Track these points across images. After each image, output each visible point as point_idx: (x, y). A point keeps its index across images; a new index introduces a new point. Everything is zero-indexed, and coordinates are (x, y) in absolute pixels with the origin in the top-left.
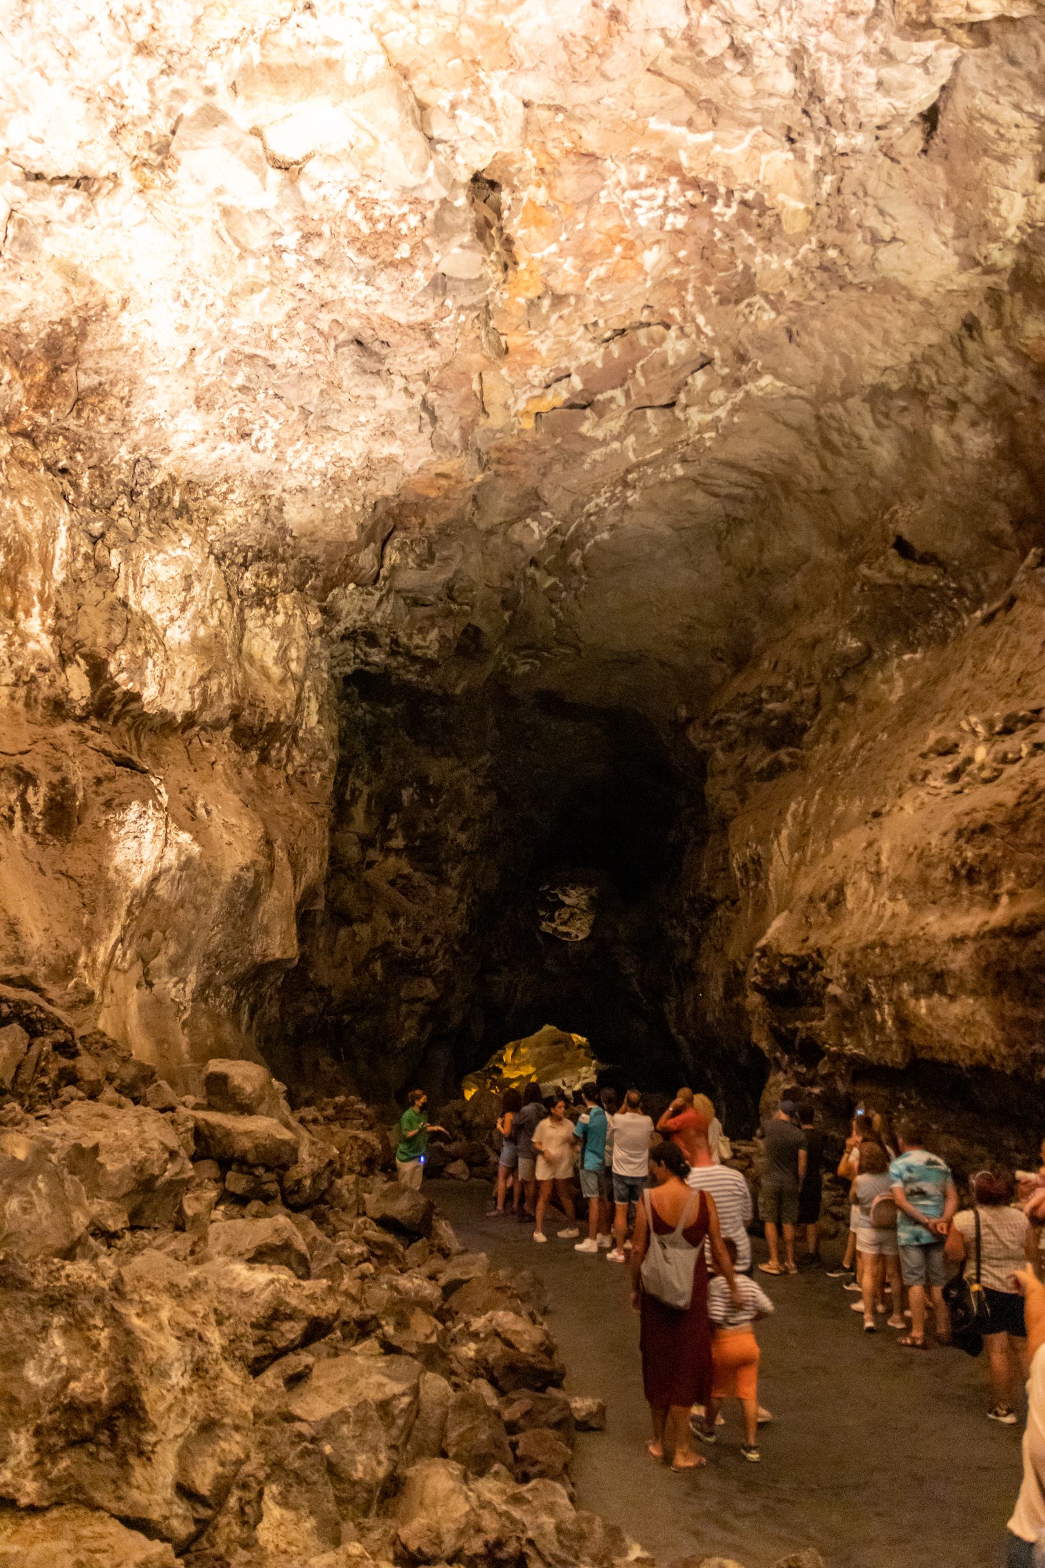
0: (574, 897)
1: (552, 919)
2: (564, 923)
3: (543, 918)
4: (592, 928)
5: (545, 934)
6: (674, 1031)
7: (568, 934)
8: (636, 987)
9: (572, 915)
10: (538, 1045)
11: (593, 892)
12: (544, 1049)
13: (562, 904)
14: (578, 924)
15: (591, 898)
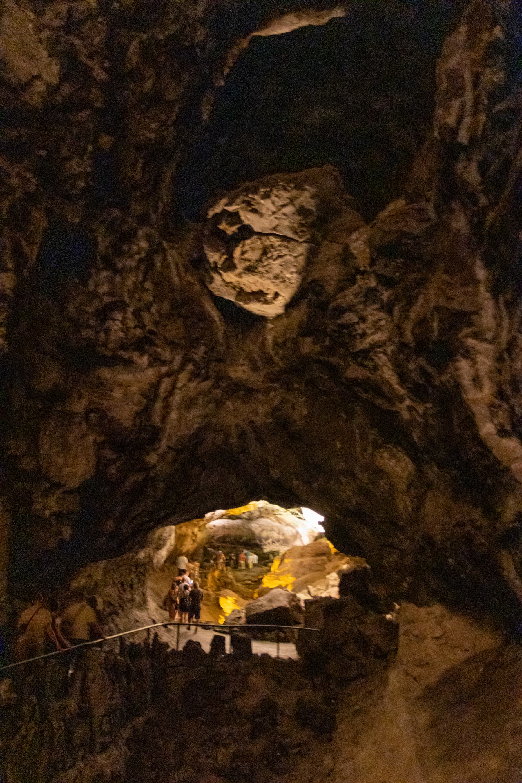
0: (271, 213)
1: (230, 266)
2: (251, 270)
3: (215, 269)
4: (304, 271)
5: (219, 302)
6: (487, 429)
7: (259, 296)
8: (388, 374)
9: (265, 251)
10: (302, 556)
11: (306, 198)
12: (307, 560)
13: (246, 232)
14: (276, 266)
15: (301, 211)
